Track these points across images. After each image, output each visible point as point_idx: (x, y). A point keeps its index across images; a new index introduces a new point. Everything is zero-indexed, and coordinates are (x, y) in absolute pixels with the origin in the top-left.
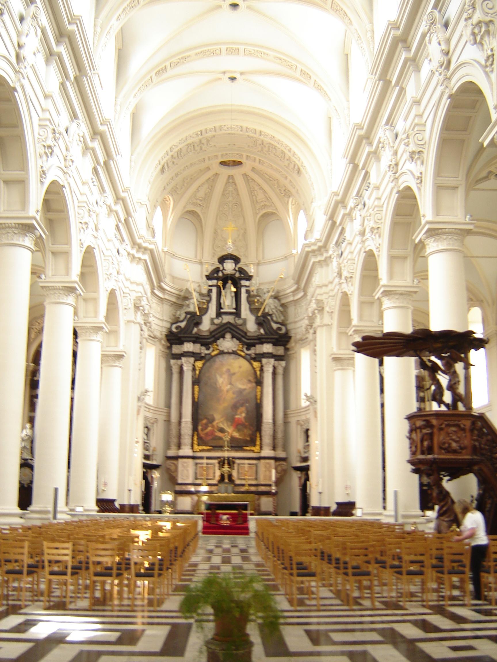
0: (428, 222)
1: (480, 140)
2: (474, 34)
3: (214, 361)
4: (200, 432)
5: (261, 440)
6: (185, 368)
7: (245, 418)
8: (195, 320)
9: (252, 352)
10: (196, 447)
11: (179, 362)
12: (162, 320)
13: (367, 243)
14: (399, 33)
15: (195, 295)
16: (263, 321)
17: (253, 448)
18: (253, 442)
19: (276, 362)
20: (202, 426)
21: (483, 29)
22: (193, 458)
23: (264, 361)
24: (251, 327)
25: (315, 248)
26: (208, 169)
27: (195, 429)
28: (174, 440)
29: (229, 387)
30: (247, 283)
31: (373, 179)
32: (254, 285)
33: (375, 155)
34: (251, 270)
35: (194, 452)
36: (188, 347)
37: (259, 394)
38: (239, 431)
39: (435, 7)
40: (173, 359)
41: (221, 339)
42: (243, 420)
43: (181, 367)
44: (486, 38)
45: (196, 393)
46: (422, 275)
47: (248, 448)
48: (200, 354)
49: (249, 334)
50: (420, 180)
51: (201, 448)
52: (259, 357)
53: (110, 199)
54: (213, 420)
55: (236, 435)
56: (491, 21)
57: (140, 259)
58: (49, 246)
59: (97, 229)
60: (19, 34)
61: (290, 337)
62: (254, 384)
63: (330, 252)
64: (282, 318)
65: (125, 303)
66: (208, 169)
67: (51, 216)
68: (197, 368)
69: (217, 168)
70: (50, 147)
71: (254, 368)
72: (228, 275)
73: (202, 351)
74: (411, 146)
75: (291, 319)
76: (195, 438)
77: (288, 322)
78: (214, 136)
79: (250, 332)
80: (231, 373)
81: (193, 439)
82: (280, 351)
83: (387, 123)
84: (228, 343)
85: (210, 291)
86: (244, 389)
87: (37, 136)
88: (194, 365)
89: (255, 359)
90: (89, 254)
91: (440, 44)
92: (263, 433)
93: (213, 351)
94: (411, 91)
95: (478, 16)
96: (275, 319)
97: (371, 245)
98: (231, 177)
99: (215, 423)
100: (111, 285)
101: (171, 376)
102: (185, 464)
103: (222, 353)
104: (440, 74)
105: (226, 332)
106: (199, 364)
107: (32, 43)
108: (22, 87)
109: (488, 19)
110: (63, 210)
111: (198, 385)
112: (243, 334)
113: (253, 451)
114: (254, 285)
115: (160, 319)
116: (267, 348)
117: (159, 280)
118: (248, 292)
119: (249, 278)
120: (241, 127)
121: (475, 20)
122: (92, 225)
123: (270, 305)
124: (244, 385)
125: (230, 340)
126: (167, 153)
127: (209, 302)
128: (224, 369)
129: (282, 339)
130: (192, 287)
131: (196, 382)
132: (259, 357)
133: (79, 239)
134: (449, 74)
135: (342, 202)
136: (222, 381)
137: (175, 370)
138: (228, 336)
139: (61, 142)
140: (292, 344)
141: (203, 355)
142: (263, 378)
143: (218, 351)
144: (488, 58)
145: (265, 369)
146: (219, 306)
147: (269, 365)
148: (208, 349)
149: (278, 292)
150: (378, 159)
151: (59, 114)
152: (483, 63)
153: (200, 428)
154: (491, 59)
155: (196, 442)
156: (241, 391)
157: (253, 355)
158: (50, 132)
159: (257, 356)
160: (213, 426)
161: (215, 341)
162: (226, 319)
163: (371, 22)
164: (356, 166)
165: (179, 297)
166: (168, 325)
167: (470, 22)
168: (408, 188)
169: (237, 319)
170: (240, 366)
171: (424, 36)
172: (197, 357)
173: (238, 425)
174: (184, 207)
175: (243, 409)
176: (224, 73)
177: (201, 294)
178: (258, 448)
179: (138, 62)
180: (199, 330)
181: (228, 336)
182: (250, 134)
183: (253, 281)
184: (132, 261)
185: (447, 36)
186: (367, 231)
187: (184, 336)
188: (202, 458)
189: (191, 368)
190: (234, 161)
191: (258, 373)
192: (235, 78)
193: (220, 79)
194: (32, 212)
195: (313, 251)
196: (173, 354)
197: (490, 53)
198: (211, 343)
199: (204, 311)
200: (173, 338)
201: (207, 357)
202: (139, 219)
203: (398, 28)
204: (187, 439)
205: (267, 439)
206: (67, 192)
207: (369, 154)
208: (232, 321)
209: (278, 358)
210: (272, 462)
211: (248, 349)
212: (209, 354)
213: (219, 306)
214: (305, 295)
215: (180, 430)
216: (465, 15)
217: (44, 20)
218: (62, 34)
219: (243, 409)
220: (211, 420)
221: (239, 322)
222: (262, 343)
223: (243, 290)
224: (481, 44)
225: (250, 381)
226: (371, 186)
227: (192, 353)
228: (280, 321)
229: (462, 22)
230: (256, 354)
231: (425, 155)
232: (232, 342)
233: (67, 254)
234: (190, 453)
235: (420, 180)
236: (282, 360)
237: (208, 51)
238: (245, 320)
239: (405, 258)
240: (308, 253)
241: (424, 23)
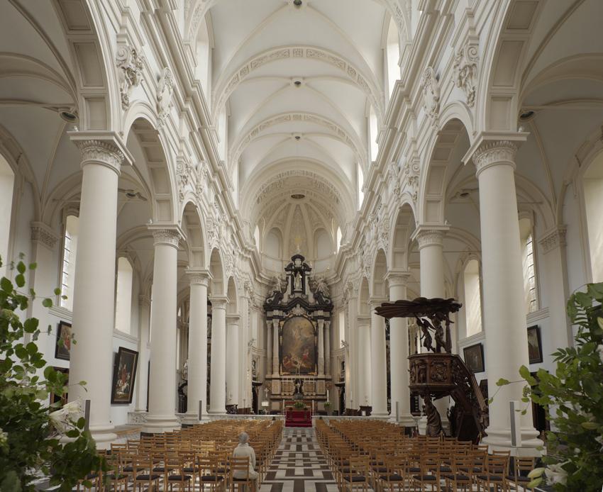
0: (421, 226)
1: (462, 161)
2: (460, 78)
6: (274, 325)
8: (279, 296)
10: (281, 372)
12: (261, 296)
13: (379, 244)
14: (404, 90)
15: (279, 281)
16: (318, 296)
21: (468, 73)
22: (281, 379)
23: (319, 320)
24: (311, 300)
25: (348, 249)
26: (285, 200)
27: (281, 362)
28: (269, 369)
29: (299, 337)
30: (308, 273)
31: (383, 201)
32: (312, 274)
33: (385, 184)
34: (311, 265)
36: (276, 312)
38: (305, 363)
39: (430, 65)
43: (272, 325)
44: (469, 80)
46: (415, 264)
50: (415, 197)
52: (316, 319)
53: (227, 218)
54: (291, 357)
55: (303, 365)
56: (474, 65)
57: (247, 258)
58: (190, 247)
59: (220, 238)
60: (157, 90)
61: (333, 306)
63: (357, 252)
65: (239, 285)
66: (285, 200)
67: (191, 227)
69: (289, 200)
70: (184, 177)
72: (298, 269)
74: (410, 173)
75: (334, 295)
78: (287, 178)
80: (300, 327)
82: (327, 314)
83: (393, 161)
84: (298, 310)
85: (287, 278)
87: (176, 169)
89: (313, 320)
90: (215, 252)
91: (433, 93)
94: (410, 134)
95: (465, 61)
97: (382, 246)
98: (298, 206)
100: (230, 274)
101: (267, 330)
103: (295, 316)
104: (432, 117)
106: (282, 323)
107: (167, 97)
108: (163, 130)
109: (472, 63)
110: (198, 223)
114: (312, 274)
115: (260, 296)
116: (320, 313)
117: (259, 272)
118: (309, 278)
119: (310, 270)
120: (303, 171)
121: (462, 66)
122: (216, 233)
123: (322, 287)
124: (307, 335)
126: (260, 190)
127: (287, 285)
128: (296, 326)
129: (329, 308)
130: (277, 275)
131: (281, 334)
132: (316, 319)
133: (209, 243)
134: (438, 116)
135: (364, 219)
136: (295, 333)
137: (269, 326)
138: (298, 306)
139: (192, 173)
140: (334, 310)
144: (470, 95)
145: (319, 325)
146: (293, 287)
147: (321, 323)
149: (326, 278)
150: (387, 187)
151: (190, 155)
152: (465, 100)
154: (472, 96)
155: (281, 370)
156: (306, 339)
158: (184, 166)
161: (291, 309)
162: (297, 295)
163: (383, 91)
164: (373, 193)
165: (270, 282)
166: (265, 299)
167: (458, 68)
168: (407, 205)
170: (305, 323)
171: (422, 88)
172: (281, 318)
173: (304, 360)
174: (272, 225)
175: (307, 350)
176: (292, 134)
177: (282, 280)
179: (240, 125)
180: (282, 302)
181: (298, 306)
182: (308, 176)
183: (312, 272)
184: (242, 259)
185: (439, 86)
186: (379, 236)
187: (273, 307)
188: (285, 379)
190: (300, 195)
192: (299, 138)
193: (290, 138)
194: (176, 222)
195: (346, 252)
197: (472, 91)
199: (284, 290)
200: (267, 307)
202: (245, 231)
203: (404, 86)
205: (321, 368)
206: (199, 210)
207: (381, 183)
208: (300, 297)
209: (326, 319)
210: (324, 381)
211: (310, 314)
213: (293, 287)
214: (341, 280)
215: (272, 363)
216: (454, 63)
217: (174, 81)
218: (188, 95)
219: (307, 350)
220: (290, 357)
221: (304, 297)
222: (317, 310)
223: (306, 277)
224: (465, 85)
225: (311, 333)
226: (382, 206)
229: (452, 70)
231: (419, 179)
233: (202, 252)
234: (278, 377)
235: (415, 197)
237: (283, 118)
238: (307, 296)
239: (403, 253)
240: (343, 253)
241: (422, 78)
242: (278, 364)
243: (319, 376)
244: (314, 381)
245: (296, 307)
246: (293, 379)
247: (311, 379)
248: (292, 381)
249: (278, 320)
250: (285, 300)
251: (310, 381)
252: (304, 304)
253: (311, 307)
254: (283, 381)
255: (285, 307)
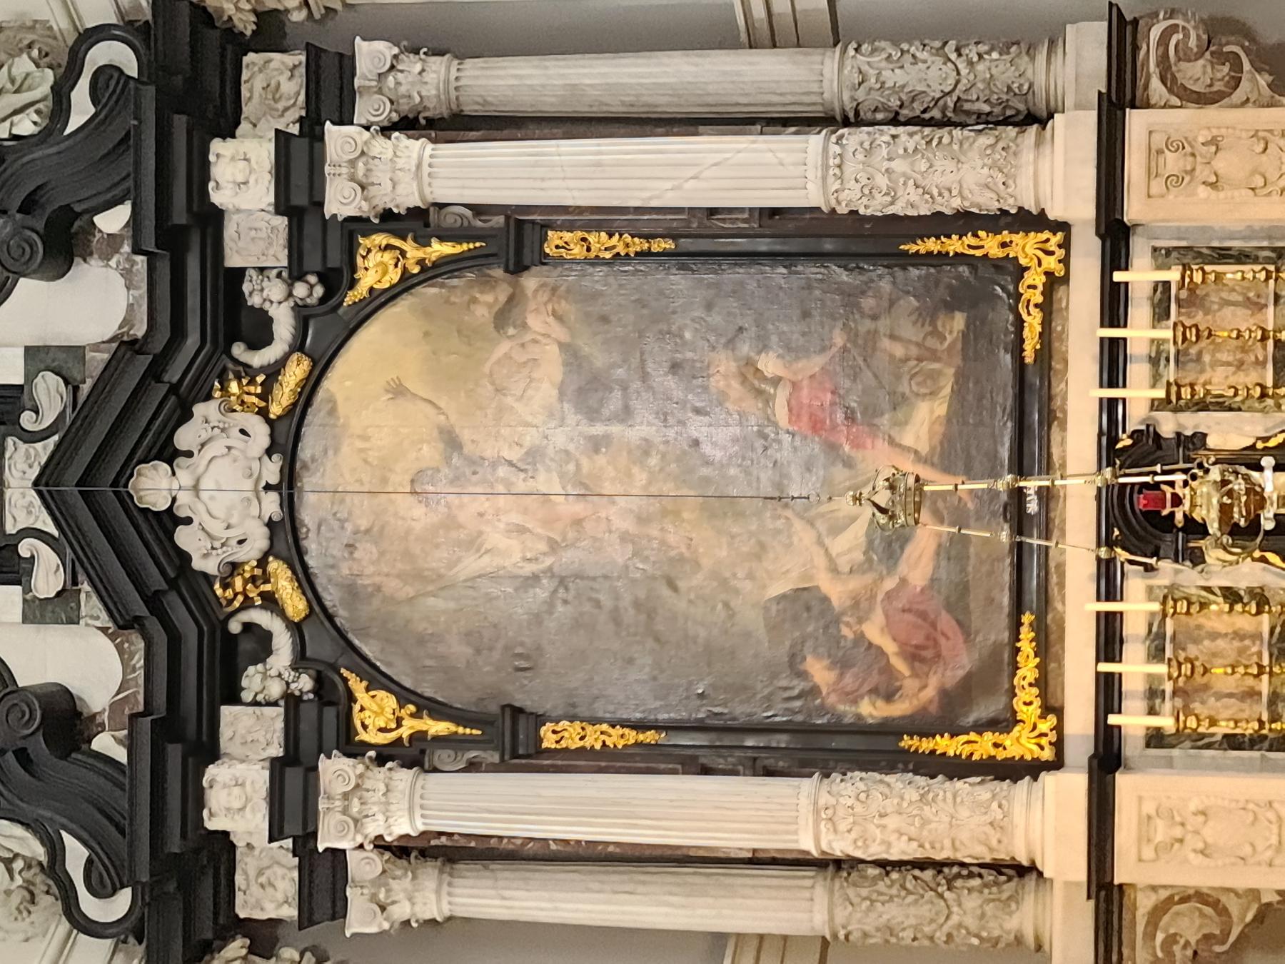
3: (352, 591)
4: (899, 709)
5: (966, 221)
6: (401, 826)
7: (791, 351)
9: (273, 299)
10: (1020, 744)
11: (363, 866)
17: (1035, 278)
18: (979, 289)
19: (364, 109)
20: (855, 702)
22: (1107, 758)
23: (340, 201)
24: (93, 303)
29: (547, 481)
35: (1057, 764)
36: (235, 796)
37: (598, 240)
40: (339, 910)
41: (184, 537)
42: (816, 363)
43: (401, 851)
45: (594, 738)
47: (1033, 322)
48: (292, 701)
49: (140, 330)
51: (1027, 705)
55: (924, 421)
62: (530, 282)
64: (23, 65)
68: (410, 727)
71: (406, 284)
73: (275, 690)
76: (946, 745)
77: (60, 22)
79: (127, 322)
81: (959, 768)
82: (273, 82)
84: (213, 487)
86: (572, 356)
88: (383, 756)
89: (337, 279)
92: (911, 203)
93: (271, 602)
96: (26, 126)
99: (837, 592)
102: (1161, 832)
103: (286, 536)
105: (125, 501)
106: (376, 714)
111: (540, 719)
112: (144, 362)
113: (1054, 283)
116: (241, 175)
125: (185, 477)
128: (417, 515)
131: (510, 738)
132: (322, 246)
138: (154, 486)
141: (305, 683)
142: (478, 210)
143: (274, 565)
145: (406, 197)
148: (262, 643)
153: (871, 710)
156: (587, 390)
157: (300, 290)
159: (313, 260)
160: (860, 607)
169: (27, 420)
172: (318, 726)
178: (1025, 246)
181: (154, 486)
188: (1108, 693)
189: (403, 777)
191: (439, 249)
196: (307, 918)
198: (212, 618)
201: (321, 648)
204: (958, 818)
205: (960, 174)
208: (44, 450)
209: (330, 91)
210: (1137, 122)
211: (261, 334)
212: (296, 628)
221: (50, 396)
222: (213, 219)
225: (505, 317)
227: (278, 767)
228: (45, 81)
230: (295, 273)
232: (200, 460)
234: (1068, 789)
236: (346, 64)
238: (36, 357)
242: (903, 788)
243: (1074, 199)
244: (1140, 275)
245: (169, 520)
246: (1109, 584)
247: (1114, 305)
248: (1137, 606)
249: (335, 771)
250: (89, 663)
251: (1139, 332)
252: (134, 404)
253: (167, 297)
254: (1132, 721)
255: (166, 671)
